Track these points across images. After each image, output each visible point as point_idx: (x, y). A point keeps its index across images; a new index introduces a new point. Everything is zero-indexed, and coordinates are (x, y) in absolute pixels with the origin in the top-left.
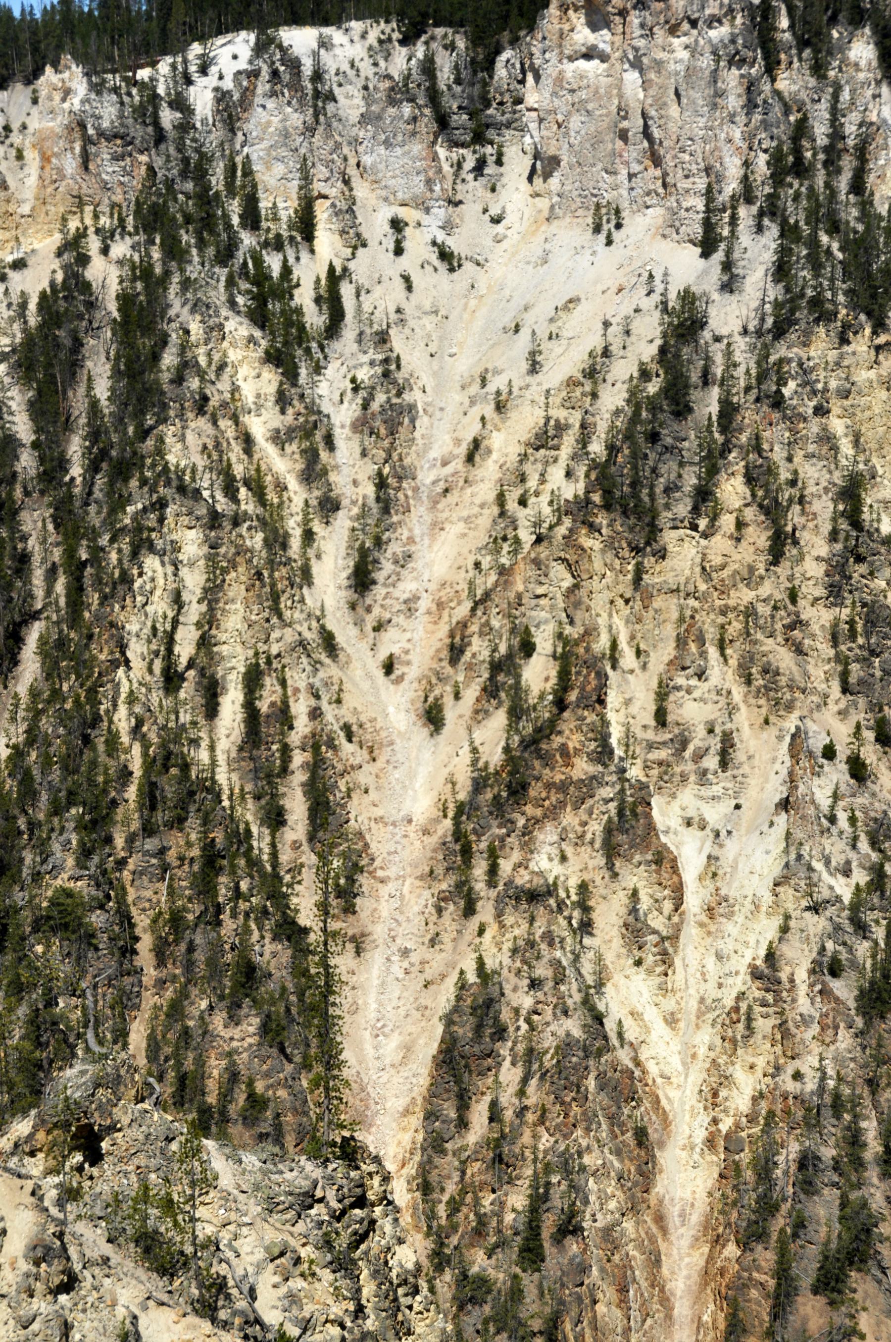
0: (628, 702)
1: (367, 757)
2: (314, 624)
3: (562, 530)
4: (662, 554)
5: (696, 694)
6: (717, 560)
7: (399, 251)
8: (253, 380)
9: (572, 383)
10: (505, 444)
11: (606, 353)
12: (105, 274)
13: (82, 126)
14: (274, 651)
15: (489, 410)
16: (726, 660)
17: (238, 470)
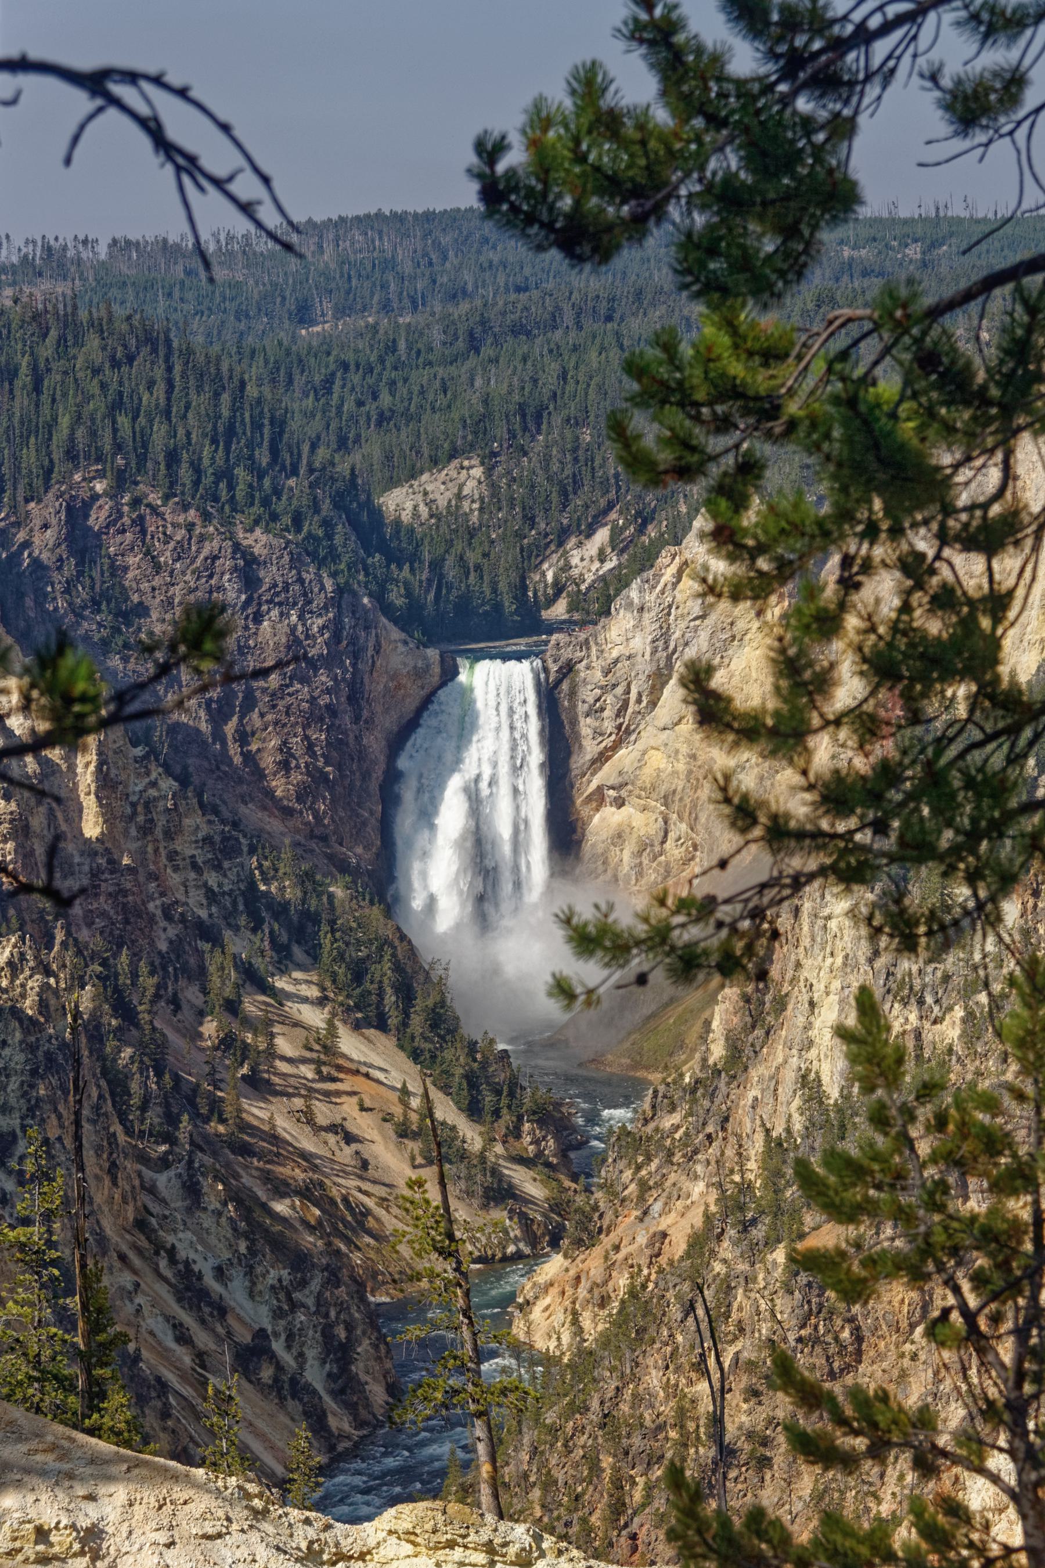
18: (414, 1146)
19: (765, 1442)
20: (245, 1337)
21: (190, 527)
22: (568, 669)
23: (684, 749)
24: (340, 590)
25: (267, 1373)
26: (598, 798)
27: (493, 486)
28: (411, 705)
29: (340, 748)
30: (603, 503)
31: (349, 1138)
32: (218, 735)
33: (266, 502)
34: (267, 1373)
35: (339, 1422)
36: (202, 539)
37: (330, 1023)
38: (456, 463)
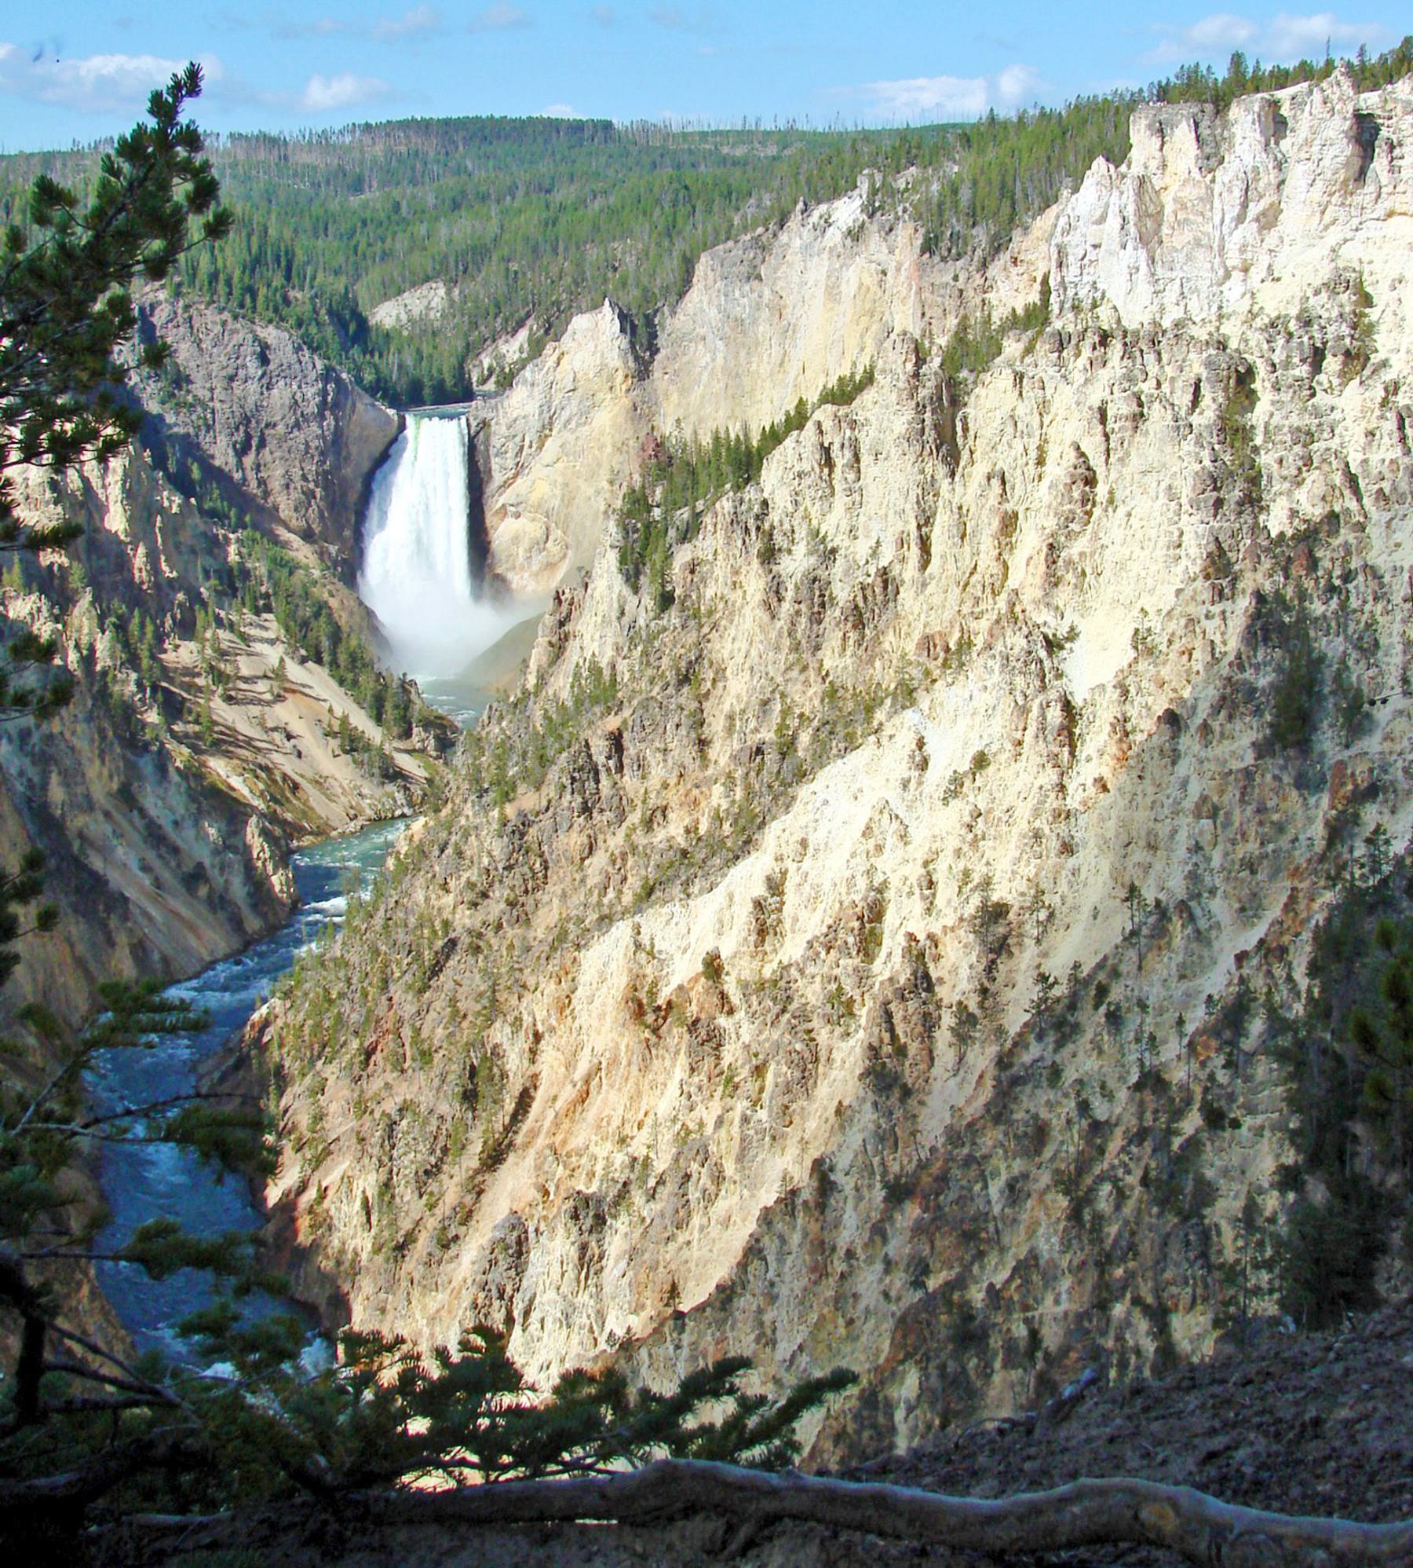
18: (334, 743)
19: (480, 936)
20: (188, 867)
21: (224, 323)
22: (485, 424)
23: (560, 480)
24: (329, 369)
25: (203, 891)
26: (503, 511)
27: (452, 302)
28: (377, 449)
29: (327, 479)
30: (523, 313)
31: (289, 737)
32: (240, 465)
33: (276, 310)
34: (203, 891)
35: (253, 924)
36: (234, 332)
37: (282, 660)
38: (426, 286)
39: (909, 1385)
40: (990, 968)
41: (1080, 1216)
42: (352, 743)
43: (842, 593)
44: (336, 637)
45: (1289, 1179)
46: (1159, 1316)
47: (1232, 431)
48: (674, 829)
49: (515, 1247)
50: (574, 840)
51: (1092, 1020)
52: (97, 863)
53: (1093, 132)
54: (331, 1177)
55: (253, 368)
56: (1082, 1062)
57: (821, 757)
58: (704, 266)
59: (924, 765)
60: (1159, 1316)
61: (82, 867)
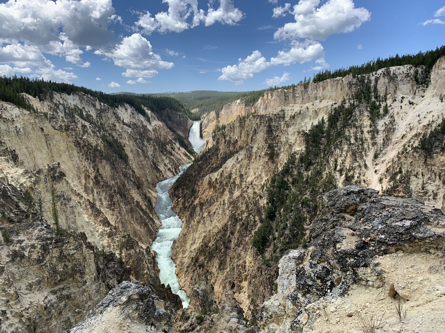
0: (418, 184)
1: (367, 185)
2: (364, 163)
3: (411, 152)
4: (432, 158)
5: (432, 185)
6: (442, 161)
7: (402, 102)
8: (367, 122)
9: (424, 126)
10: (409, 136)
11: (433, 121)
12: (347, 106)
13: (350, 83)
14: (354, 166)
15: (408, 130)
16: (440, 180)
17: (358, 137)
26: (205, 132)
39: (230, 223)
40: (241, 181)
41: (247, 207)
42: (186, 155)
43: (232, 142)
44: (185, 145)
45: (267, 203)
46: (254, 217)
47: (270, 126)
48: (214, 166)
49: (194, 208)
50: (205, 166)
51: (250, 186)
52: (159, 167)
53: (261, 94)
54: (179, 200)
55: (178, 117)
56: (250, 191)
57: (229, 158)
58: (224, 107)
59: (238, 159)
60: (254, 217)
61: (157, 168)
